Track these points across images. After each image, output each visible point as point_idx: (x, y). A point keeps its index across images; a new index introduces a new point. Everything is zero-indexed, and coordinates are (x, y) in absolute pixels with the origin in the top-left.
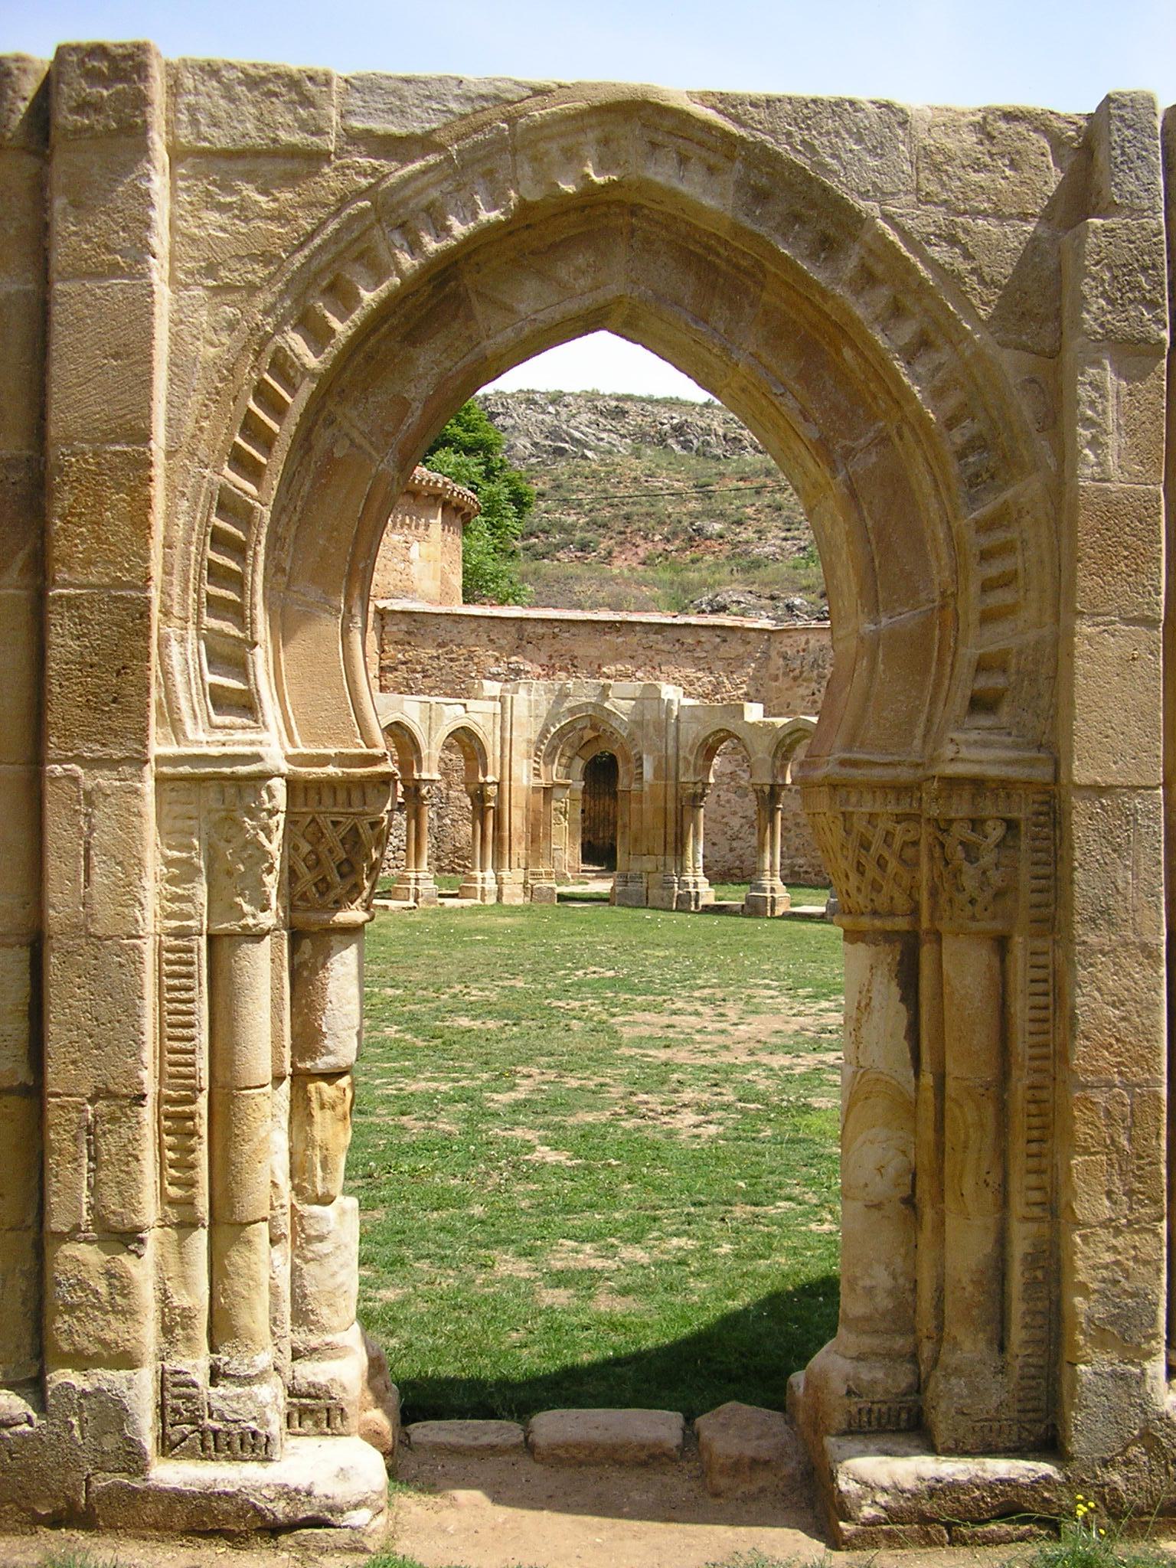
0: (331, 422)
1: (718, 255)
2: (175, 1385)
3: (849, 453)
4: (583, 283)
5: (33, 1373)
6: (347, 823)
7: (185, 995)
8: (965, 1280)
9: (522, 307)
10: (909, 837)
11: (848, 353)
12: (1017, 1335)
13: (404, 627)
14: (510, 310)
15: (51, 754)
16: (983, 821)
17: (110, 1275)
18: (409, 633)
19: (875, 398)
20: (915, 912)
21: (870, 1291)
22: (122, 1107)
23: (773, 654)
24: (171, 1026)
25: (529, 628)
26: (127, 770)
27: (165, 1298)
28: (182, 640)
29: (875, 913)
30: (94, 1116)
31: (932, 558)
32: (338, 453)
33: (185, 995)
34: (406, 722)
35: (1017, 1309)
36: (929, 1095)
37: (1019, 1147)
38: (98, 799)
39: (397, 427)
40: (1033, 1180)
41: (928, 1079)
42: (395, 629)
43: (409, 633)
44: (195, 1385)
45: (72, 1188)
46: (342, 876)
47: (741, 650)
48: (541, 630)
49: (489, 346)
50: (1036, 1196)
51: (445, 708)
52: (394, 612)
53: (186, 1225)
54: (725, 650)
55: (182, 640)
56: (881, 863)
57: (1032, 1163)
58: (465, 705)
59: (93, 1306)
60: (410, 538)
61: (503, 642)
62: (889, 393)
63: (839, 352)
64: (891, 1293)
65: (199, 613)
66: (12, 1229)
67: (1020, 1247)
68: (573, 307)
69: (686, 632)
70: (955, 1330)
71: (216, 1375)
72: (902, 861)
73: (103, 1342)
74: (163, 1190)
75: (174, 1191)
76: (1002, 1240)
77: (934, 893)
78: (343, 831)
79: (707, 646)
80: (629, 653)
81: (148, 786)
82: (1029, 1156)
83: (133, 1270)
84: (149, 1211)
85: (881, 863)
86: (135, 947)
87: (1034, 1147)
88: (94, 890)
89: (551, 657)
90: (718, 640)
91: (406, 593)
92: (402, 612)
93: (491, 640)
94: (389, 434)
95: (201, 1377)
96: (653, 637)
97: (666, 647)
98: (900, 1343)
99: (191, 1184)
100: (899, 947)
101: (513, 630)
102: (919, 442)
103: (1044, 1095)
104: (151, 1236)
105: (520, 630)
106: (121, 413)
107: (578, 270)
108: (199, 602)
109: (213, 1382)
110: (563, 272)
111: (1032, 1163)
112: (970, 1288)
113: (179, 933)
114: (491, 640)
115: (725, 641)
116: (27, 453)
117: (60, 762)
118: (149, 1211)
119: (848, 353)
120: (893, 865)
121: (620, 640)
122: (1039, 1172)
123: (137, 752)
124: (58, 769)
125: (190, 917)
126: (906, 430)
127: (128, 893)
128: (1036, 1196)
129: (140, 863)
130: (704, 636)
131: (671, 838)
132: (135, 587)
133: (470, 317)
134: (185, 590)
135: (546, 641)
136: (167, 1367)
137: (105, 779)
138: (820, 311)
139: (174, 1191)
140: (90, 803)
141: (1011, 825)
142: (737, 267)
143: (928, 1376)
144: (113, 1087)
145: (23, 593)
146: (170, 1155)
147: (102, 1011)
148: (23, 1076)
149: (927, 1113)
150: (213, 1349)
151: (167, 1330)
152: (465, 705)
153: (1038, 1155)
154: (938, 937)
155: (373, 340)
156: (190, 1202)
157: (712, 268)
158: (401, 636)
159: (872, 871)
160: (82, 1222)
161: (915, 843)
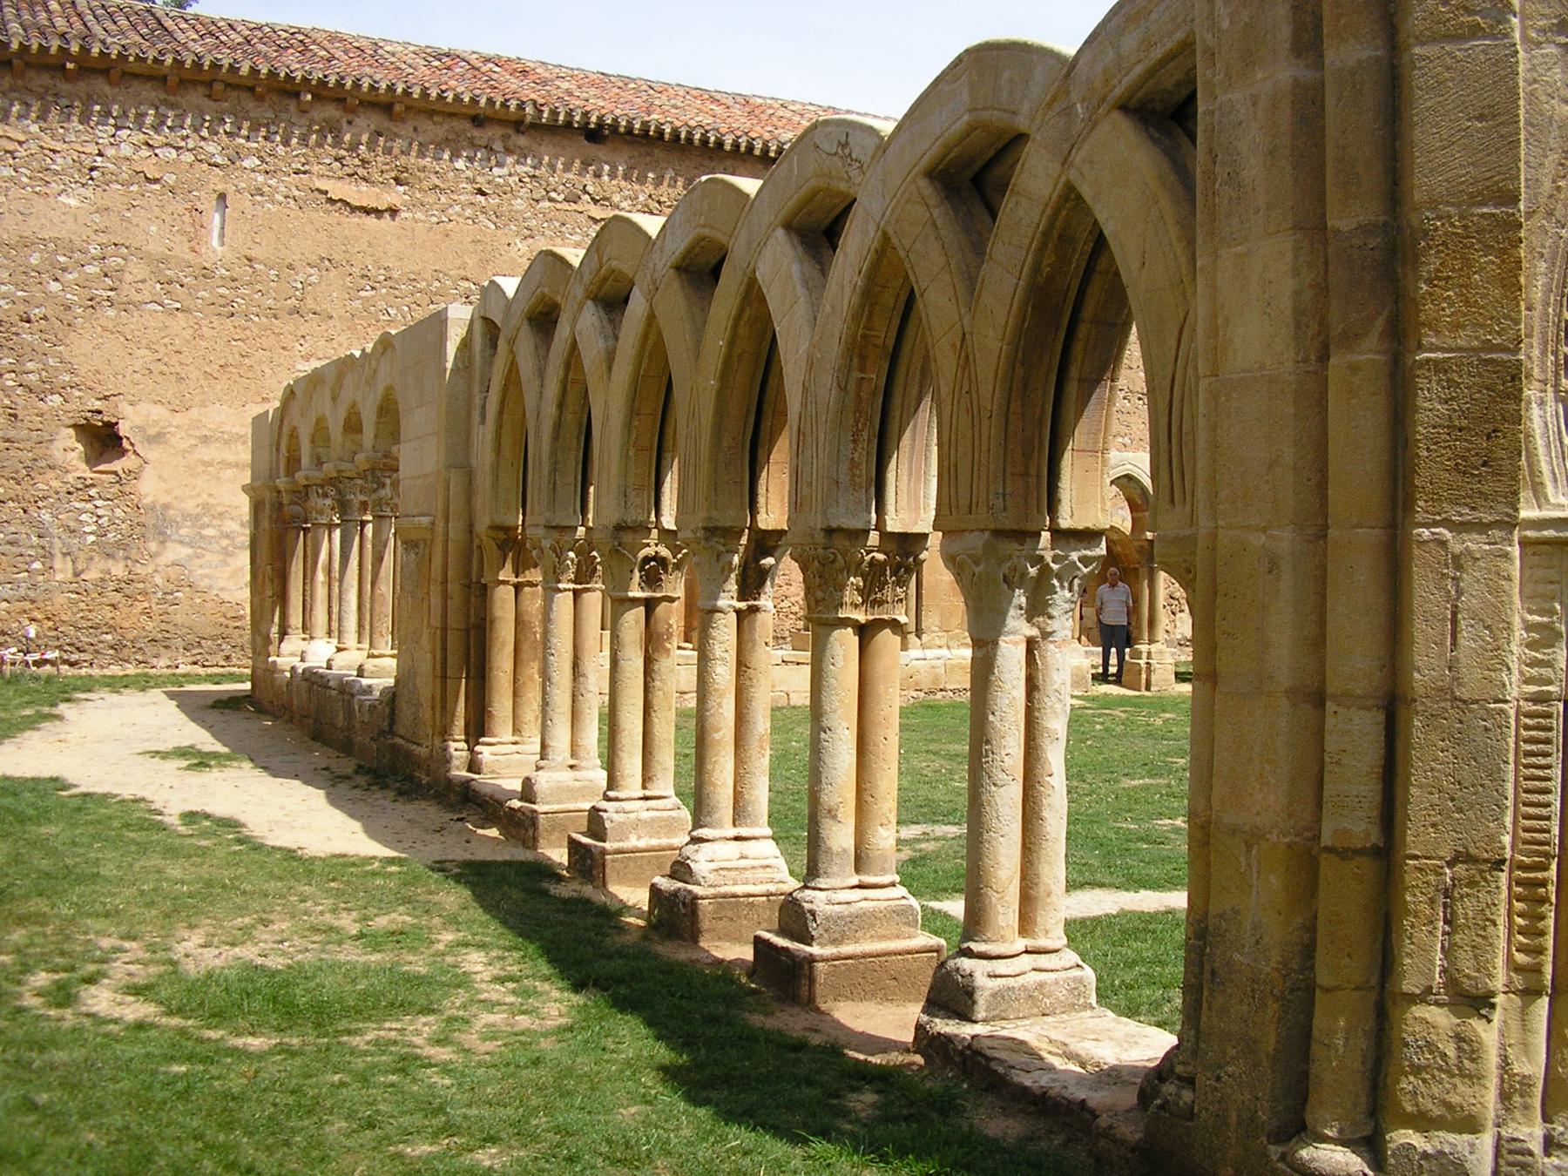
2: (1510, 1152)
5: (1367, 1131)
7: (1542, 761)
15: (1419, 518)
17: (1459, 1038)
22: (1481, 872)
24: (1527, 791)
26: (1497, 533)
27: (1505, 1063)
28: (1542, 403)
30: (1453, 879)
33: (1542, 761)
38: (1467, 562)
44: (1531, 1154)
45: (1427, 950)
53: (1530, 993)
55: (1542, 403)
59: (1440, 1069)
65: (1557, 374)
66: (1357, 988)
71: (1550, 1144)
73: (1448, 1106)
74: (1509, 956)
75: (1520, 958)
81: (1516, 551)
83: (1483, 1035)
84: (1499, 979)
86: (1502, 711)
88: (1461, 654)
95: (1536, 1146)
99: (1540, 951)
104: (1499, 999)
106: (1488, 175)
108: (1556, 364)
109: (1547, 1153)
113: (1537, 699)
116: (1383, 218)
117: (1427, 526)
118: (1499, 979)
123: (1509, 515)
124: (1426, 533)
125: (1550, 682)
127: (1495, 658)
129: (1509, 627)
132: (1506, 350)
134: (1544, 353)
136: (1504, 1133)
137: (1474, 543)
139: (1520, 958)
140: (1458, 567)
144: (1473, 851)
145: (1383, 358)
146: (1519, 921)
147: (1466, 775)
148: (1375, 838)
150: (1546, 1118)
151: (1504, 1097)
156: (1537, 970)
160: (1435, 985)
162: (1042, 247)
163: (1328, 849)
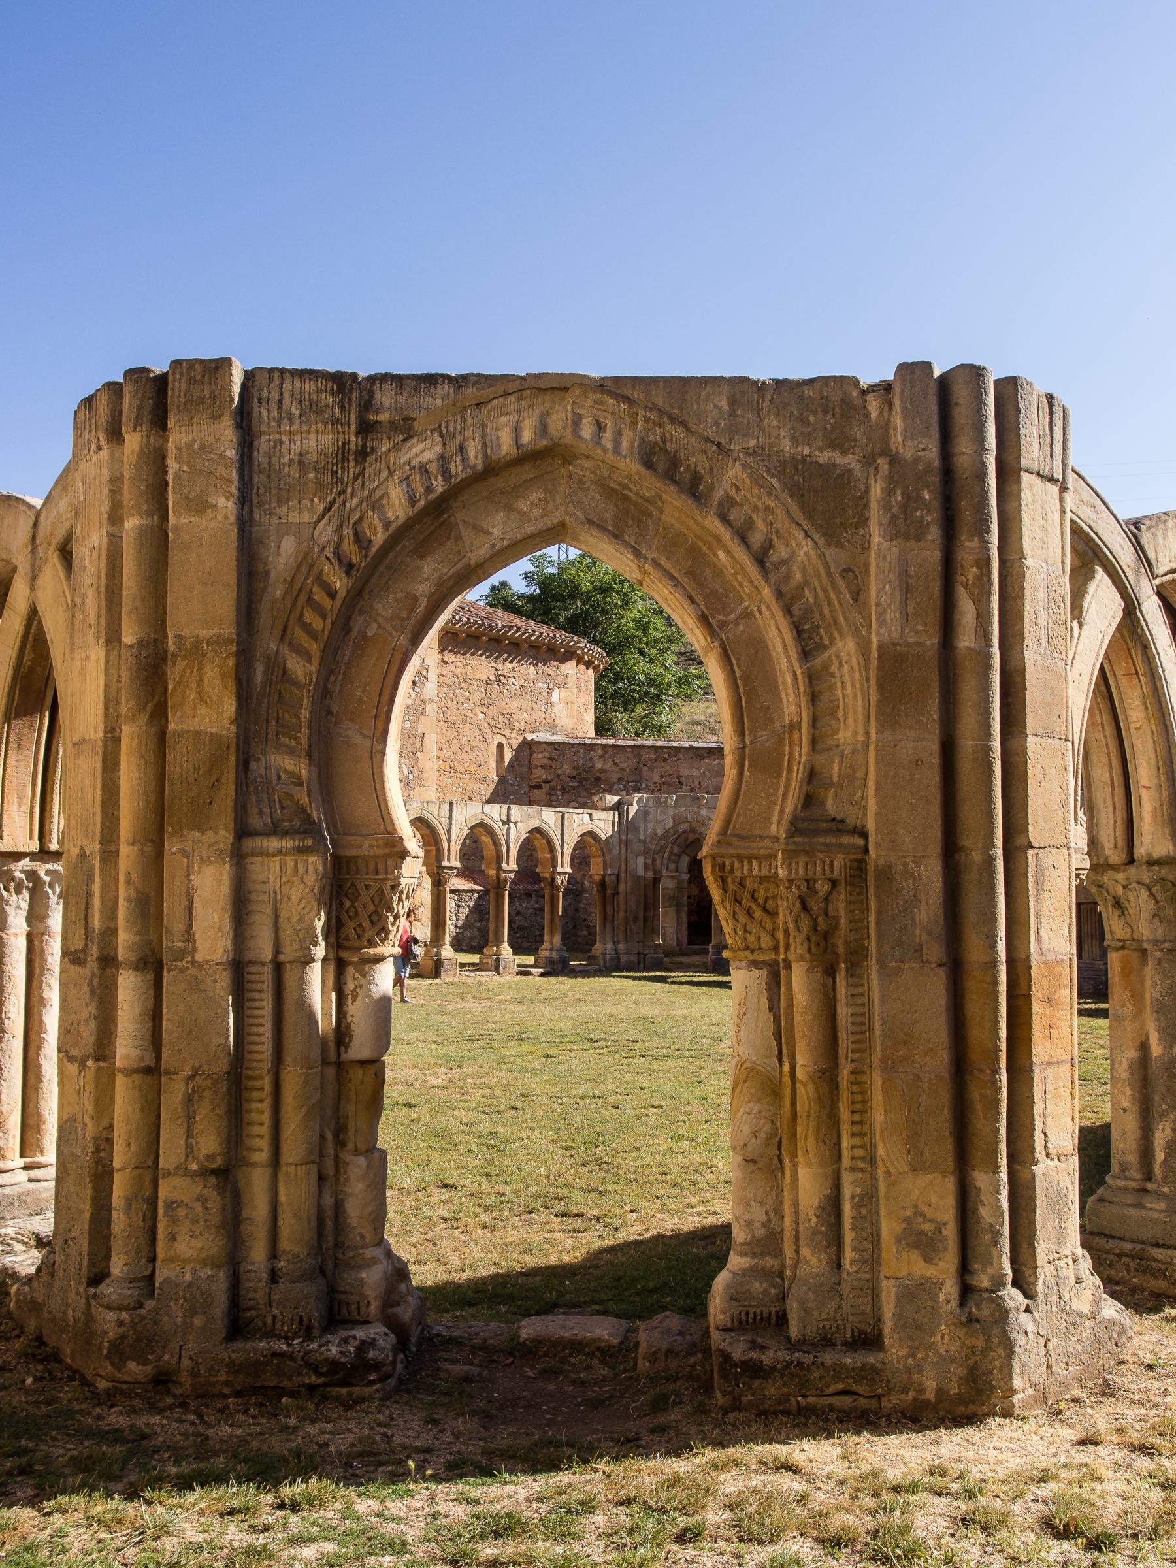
0: (362, 612)
1: (630, 490)
3: (722, 625)
4: (536, 512)
6: (375, 886)
8: (811, 1213)
9: (496, 531)
10: (769, 894)
11: (722, 555)
12: (848, 1255)
14: (487, 533)
16: (815, 881)
18: (551, 759)
19: (741, 585)
20: (776, 948)
21: (749, 1224)
29: (747, 948)
31: (783, 696)
32: (369, 634)
34: (544, 827)
35: (848, 1236)
36: (787, 1079)
37: (845, 1115)
39: (409, 617)
40: (857, 1141)
41: (786, 1067)
42: (540, 756)
46: (372, 922)
49: (474, 557)
50: (860, 1152)
51: (575, 816)
52: (539, 743)
56: (749, 913)
57: (856, 1128)
58: (590, 815)
60: (551, 686)
61: (624, 765)
62: (751, 582)
63: (715, 554)
64: (764, 1225)
67: (847, 1191)
68: (530, 529)
70: (806, 1252)
72: (765, 910)
76: (837, 1186)
77: (786, 933)
78: (372, 891)
82: (853, 1123)
85: (749, 913)
87: (857, 1117)
89: (662, 777)
92: (546, 743)
94: (403, 620)
98: (770, 1262)
100: (765, 972)
102: (773, 615)
103: (865, 1078)
105: (638, 756)
107: (532, 503)
110: (523, 505)
111: (856, 1128)
112: (814, 1220)
114: (615, 764)
119: (722, 555)
120: (758, 913)
122: (861, 1135)
126: (764, 608)
128: (860, 1152)
133: (459, 538)
138: (703, 527)
141: (834, 883)
142: (643, 497)
143: (789, 1288)
148: (149, 1061)
149: (787, 1092)
152: (590, 815)
153: (861, 1123)
154: (788, 966)
155: (391, 555)
157: (626, 498)
158: (545, 761)
159: (742, 918)
161: (774, 898)
162: (22, 649)
163: (119, 1070)
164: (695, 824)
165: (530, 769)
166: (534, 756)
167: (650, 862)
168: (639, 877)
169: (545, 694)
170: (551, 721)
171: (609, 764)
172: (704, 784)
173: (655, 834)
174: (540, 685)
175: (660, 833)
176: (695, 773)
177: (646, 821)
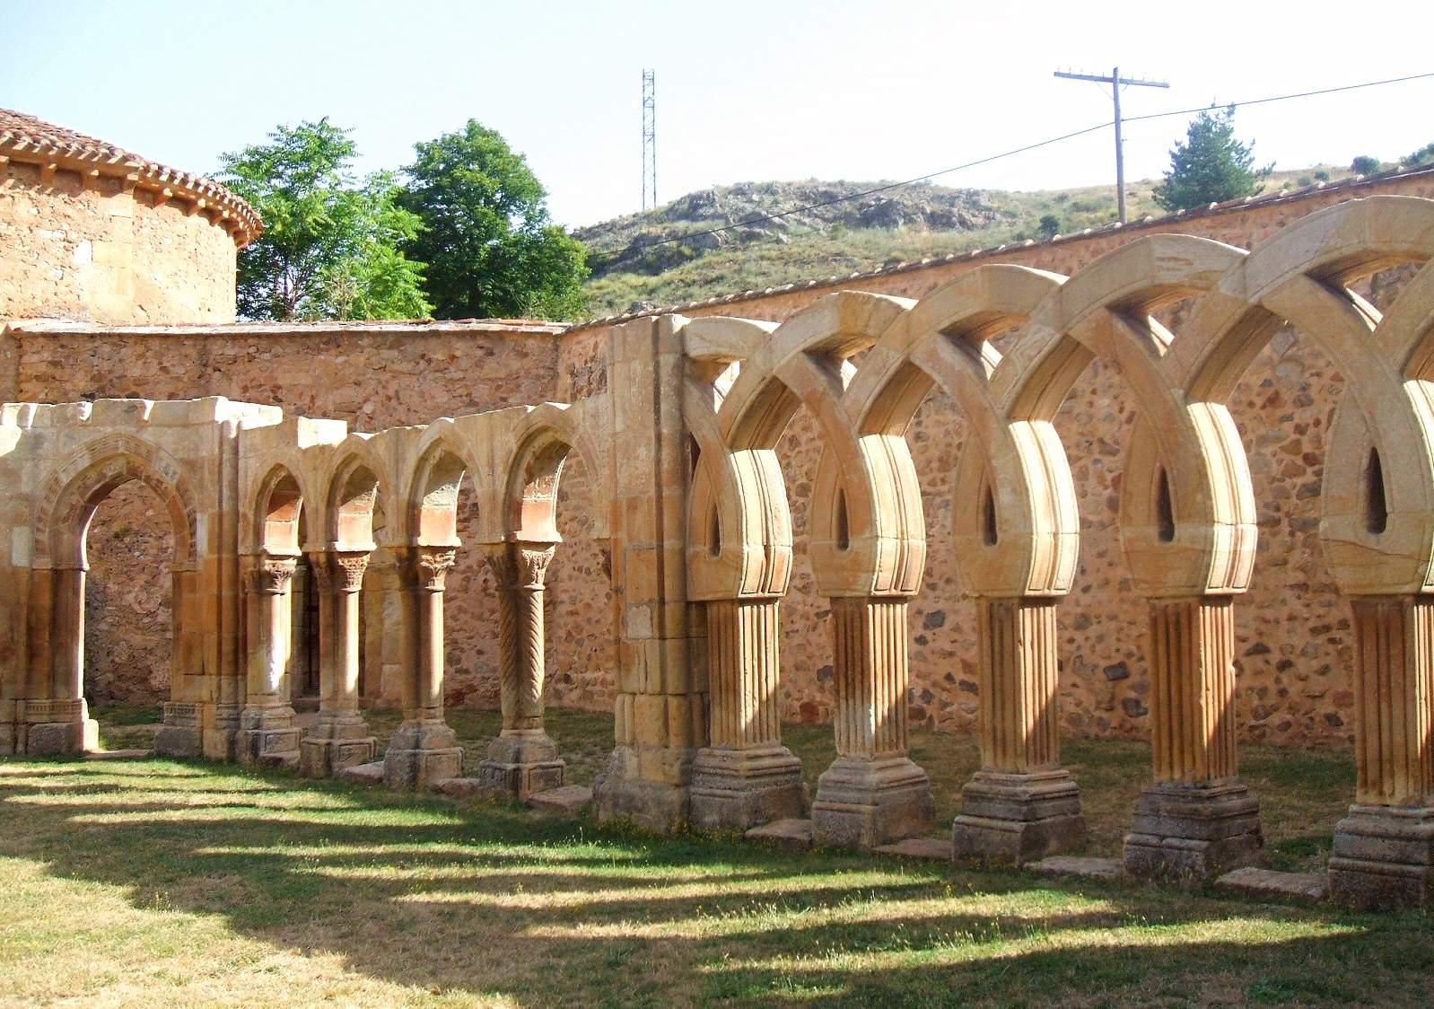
13: (46, 355)
18: (55, 364)
23: (561, 369)
25: (216, 349)
42: (35, 358)
43: (55, 364)
47: (515, 364)
48: (231, 351)
52: (33, 336)
54: (492, 368)
60: (73, 236)
61: (180, 371)
69: (433, 342)
79: (464, 363)
80: (354, 378)
90: (480, 353)
91: (65, 310)
92: (44, 335)
93: (164, 369)
96: (386, 353)
97: (406, 367)
101: (193, 353)
105: (204, 353)
114: (164, 369)
115: (491, 353)
121: (341, 359)
130: (460, 348)
131: (227, 647)
135: (240, 367)
158: (43, 368)
164: (138, 461)
165: (18, 383)
166: (25, 359)
167: (45, 537)
168: (15, 570)
169: (57, 249)
170: (71, 298)
171: (154, 369)
172: (319, 403)
173: (57, 481)
174: (44, 234)
175: (65, 480)
176: (304, 380)
177: (36, 459)
